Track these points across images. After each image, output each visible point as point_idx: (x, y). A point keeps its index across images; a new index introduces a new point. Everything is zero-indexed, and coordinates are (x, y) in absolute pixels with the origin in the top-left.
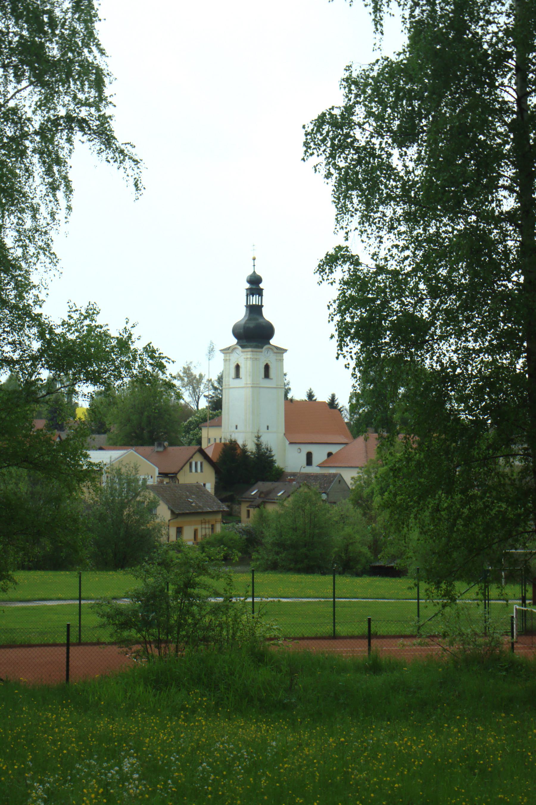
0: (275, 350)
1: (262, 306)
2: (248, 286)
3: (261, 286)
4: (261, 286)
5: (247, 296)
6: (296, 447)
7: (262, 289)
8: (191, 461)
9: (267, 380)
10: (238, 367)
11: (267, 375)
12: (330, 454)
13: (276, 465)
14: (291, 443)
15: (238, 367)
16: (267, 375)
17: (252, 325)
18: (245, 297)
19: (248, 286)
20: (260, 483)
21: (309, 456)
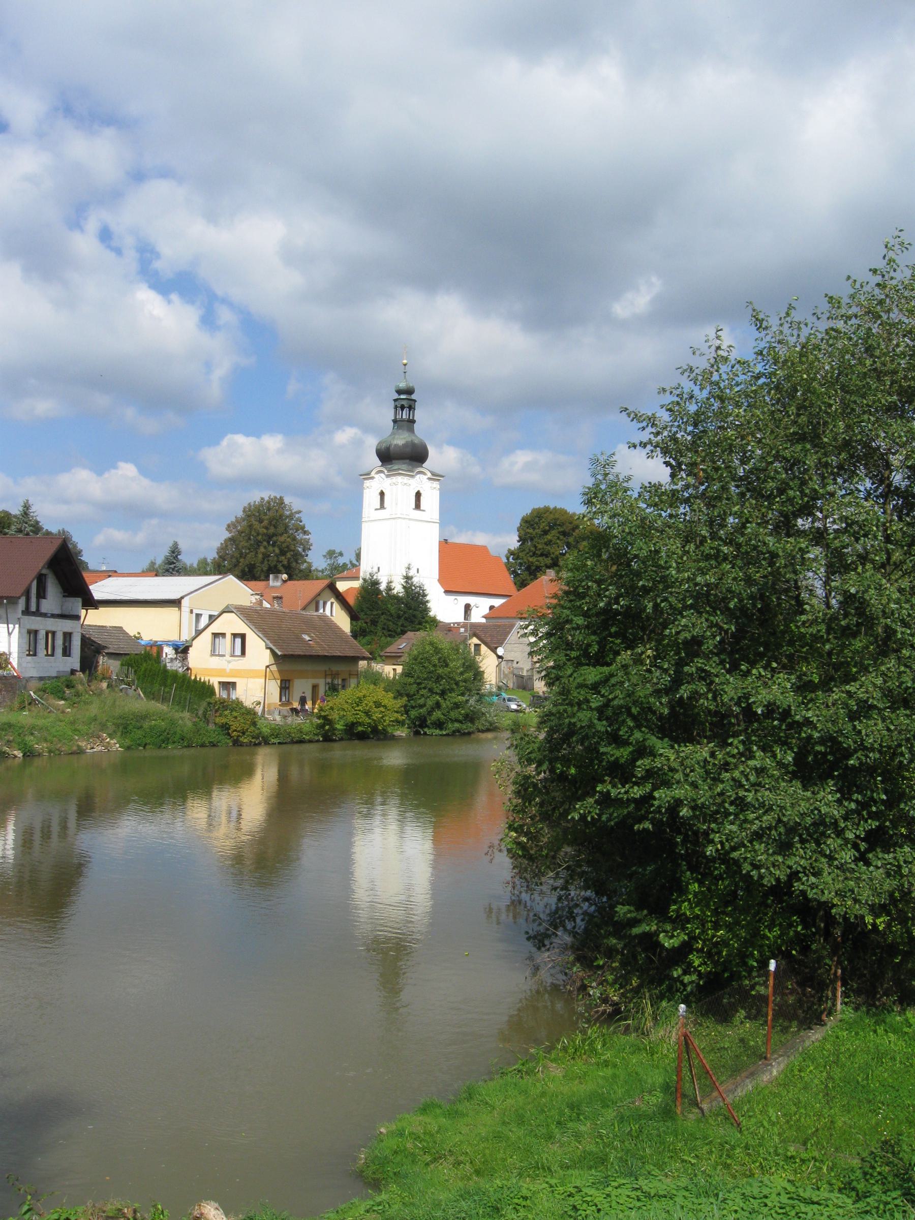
0: (429, 475)
1: (413, 422)
2: (396, 396)
3: (413, 397)
4: (413, 397)
5: (396, 407)
6: (451, 598)
7: (415, 401)
8: (318, 598)
9: (417, 512)
10: (382, 494)
11: (418, 506)
12: (492, 608)
13: (432, 614)
14: (447, 592)
15: (382, 494)
16: (418, 506)
17: (401, 440)
18: (393, 411)
19: (396, 396)
20: (410, 634)
21: (468, 608)
